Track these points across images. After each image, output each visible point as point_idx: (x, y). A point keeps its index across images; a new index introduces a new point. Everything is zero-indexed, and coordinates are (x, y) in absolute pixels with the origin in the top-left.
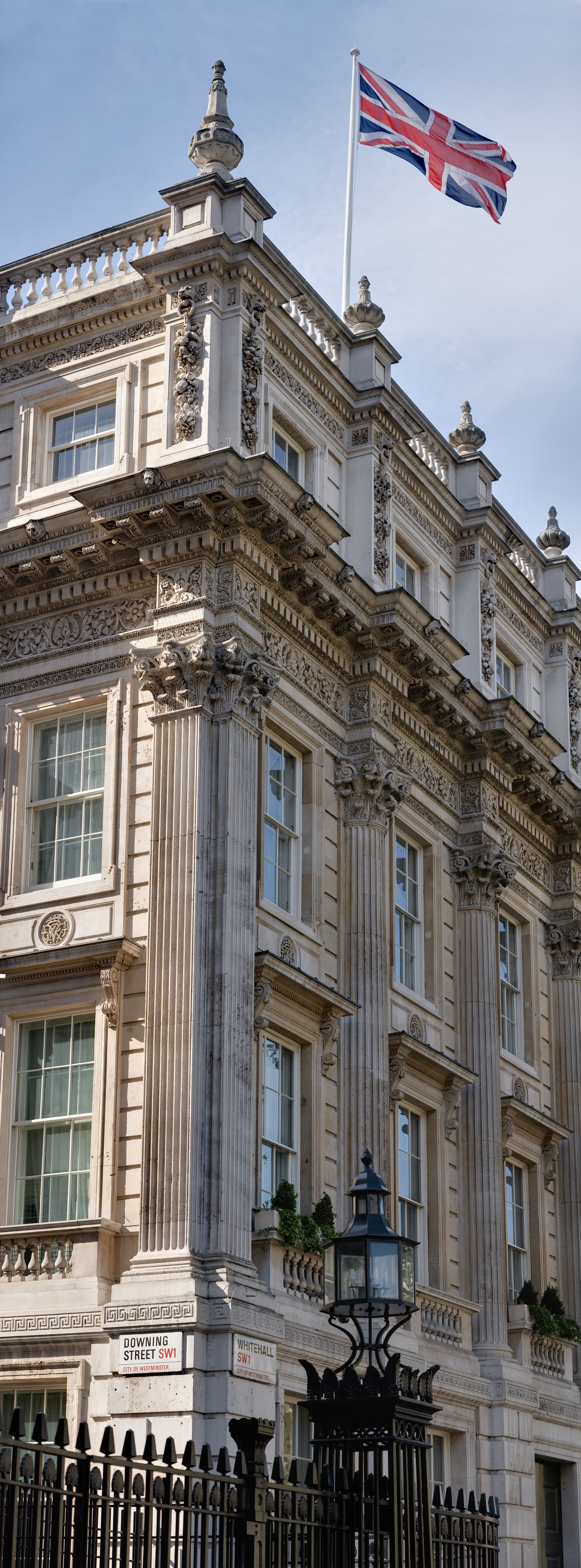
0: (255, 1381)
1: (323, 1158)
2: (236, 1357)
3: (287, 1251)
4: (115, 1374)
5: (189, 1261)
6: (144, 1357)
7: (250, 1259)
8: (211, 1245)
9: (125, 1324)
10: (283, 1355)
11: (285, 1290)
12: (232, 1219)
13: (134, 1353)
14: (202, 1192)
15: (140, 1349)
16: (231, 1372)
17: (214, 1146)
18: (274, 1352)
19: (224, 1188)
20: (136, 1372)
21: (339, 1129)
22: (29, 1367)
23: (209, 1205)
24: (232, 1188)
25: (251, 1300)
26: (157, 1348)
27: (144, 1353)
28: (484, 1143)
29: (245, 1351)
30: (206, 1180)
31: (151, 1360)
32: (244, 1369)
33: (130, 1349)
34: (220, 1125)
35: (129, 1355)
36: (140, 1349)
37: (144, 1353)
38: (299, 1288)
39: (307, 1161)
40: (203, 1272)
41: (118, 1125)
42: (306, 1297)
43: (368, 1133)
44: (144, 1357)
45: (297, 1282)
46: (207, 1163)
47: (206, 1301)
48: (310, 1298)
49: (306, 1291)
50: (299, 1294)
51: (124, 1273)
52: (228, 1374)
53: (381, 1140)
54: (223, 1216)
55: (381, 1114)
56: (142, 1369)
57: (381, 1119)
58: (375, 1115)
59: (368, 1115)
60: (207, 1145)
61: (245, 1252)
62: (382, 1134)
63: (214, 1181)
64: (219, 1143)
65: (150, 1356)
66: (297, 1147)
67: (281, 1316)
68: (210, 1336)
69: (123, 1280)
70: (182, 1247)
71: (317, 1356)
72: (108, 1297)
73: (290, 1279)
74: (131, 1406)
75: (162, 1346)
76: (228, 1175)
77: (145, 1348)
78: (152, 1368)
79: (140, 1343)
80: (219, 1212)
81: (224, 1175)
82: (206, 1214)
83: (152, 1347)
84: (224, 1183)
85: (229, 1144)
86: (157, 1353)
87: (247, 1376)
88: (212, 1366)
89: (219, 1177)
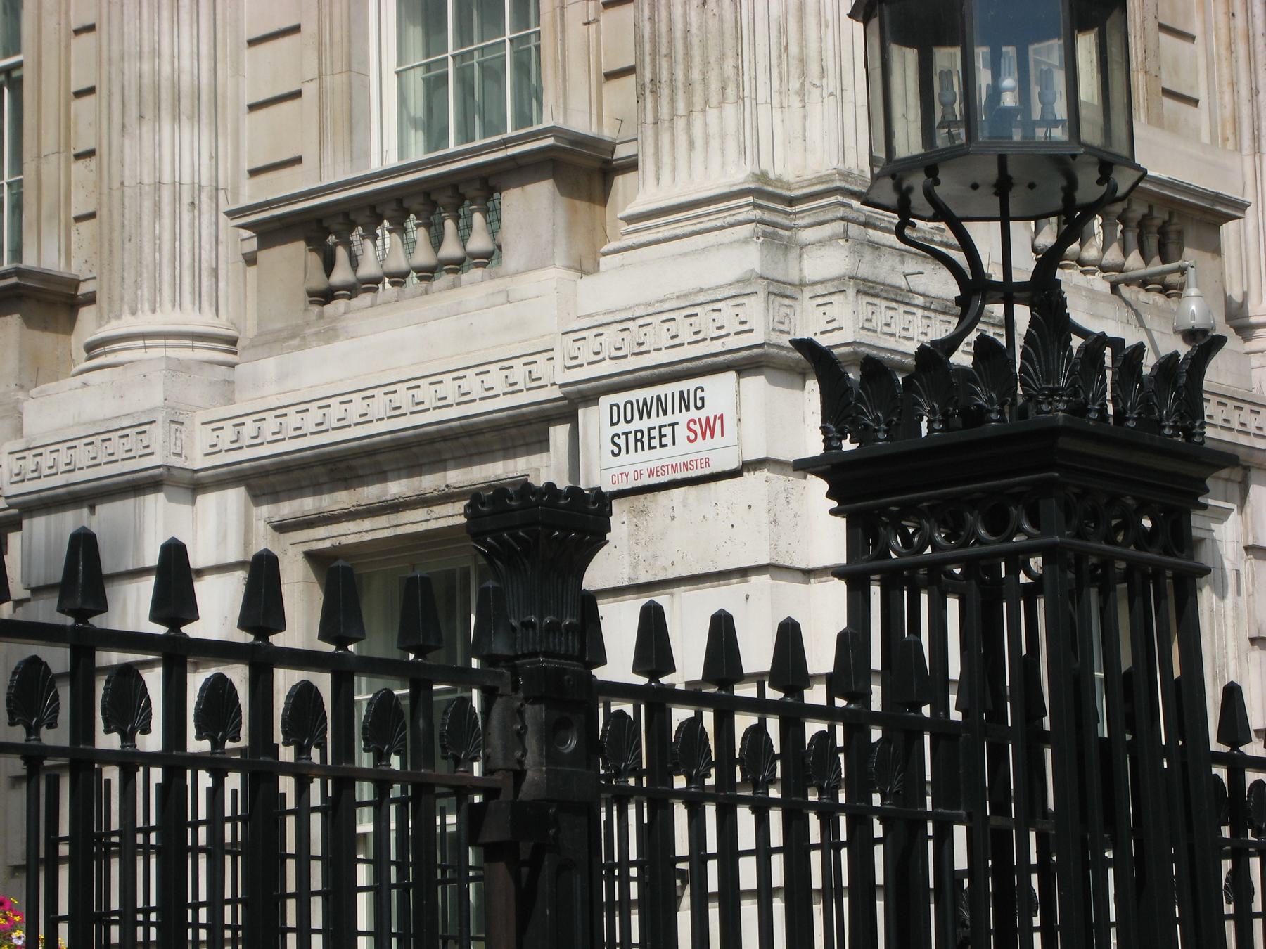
6: (655, 443)
9: (607, 368)
13: (631, 437)
15: (644, 424)
20: (639, 483)
22: (423, 501)
23: (802, 60)
25: (918, 283)
26: (682, 418)
27: (655, 433)
31: (670, 450)
33: (622, 427)
35: (622, 442)
36: (644, 424)
37: (655, 433)
44: (654, 443)
56: (651, 473)
74: (634, 567)
75: (694, 413)
77: (656, 421)
78: (674, 468)
79: (644, 409)
82: (795, 84)
86: (682, 431)
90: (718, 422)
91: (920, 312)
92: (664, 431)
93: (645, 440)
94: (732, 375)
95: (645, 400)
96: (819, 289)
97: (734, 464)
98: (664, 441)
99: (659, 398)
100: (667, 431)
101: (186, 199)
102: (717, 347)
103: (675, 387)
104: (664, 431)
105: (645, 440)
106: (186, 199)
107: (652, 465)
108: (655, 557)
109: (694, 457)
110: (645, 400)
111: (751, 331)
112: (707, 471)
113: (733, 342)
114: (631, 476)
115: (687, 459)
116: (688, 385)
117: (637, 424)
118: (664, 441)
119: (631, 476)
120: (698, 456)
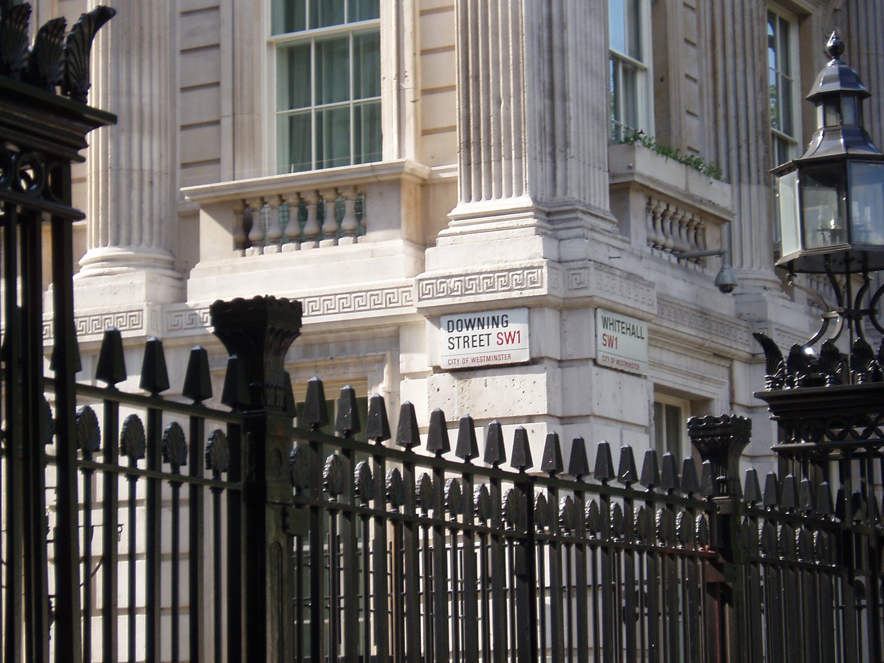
0: (622, 371)
1: (682, 76)
2: (600, 340)
3: (650, 199)
4: (437, 369)
5: (532, 213)
7: (608, 207)
8: (559, 191)
10: (657, 339)
11: (648, 250)
12: (584, 155)
13: (461, 340)
14: (542, 119)
15: (470, 332)
16: (595, 361)
17: (557, 55)
18: (645, 334)
19: (572, 112)
20: (466, 366)
21: (699, 37)
23: (553, 136)
24: (583, 112)
25: (615, 263)
26: (494, 330)
28: (873, 58)
29: (609, 332)
30: (547, 102)
32: (611, 356)
34: (563, 27)
35: (455, 342)
38: (664, 248)
39: (662, 80)
40: (549, 226)
41: (418, 32)
42: (674, 260)
43: (739, 40)
45: (661, 239)
46: (547, 79)
47: (557, 265)
48: (679, 260)
49: (673, 251)
50: (665, 256)
51: (441, 233)
52: (591, 363)
53: (756, 50)
54: (572, 151)
55: (755, 16)
56: (473, 360)
57: (755, 21)
58: (747, 17)
59: (738, 17)
60: (546, 56)
61: (601, 200)
62: (756, 42)
63: (558, 103)
64: (563, 51)
65: (484, 343)
66: (647, 61)
67: (651, 285)
68: (565, 313)
69: (440, 240)
70: (520, 193)
71: (691, 338)
72: (421, 265)
73: (653, 235)
75: (501, 329)
76: (577, 95)
77: (477, 331)
78: (489, 359)
79: (470, 325)
80: (566, 144)
81: (572, 95)
82: (548, 149)
83: (486, 330)
84: (572, 105)
85: (576, 52)
86: (493, 339)
87: (614, 366)
88: (571, 352)
89: (565, 98)
90: (517, 335)
91: (617, 278)
92: (482, 338)
93: (470, 341)
94: (525, 312)
95: (470, 320)
96: (573, 265)
97: (526, 359)
98: (482, 343)
99: (479, 319)
100: (484, 338)
101: (147, 179)
102: (515, 294)
103: (490, 314)
104: (482, 338)
105: (470, 341)
106: (147, 179)
107: (475, 356)
108: (473, 406)
109: (501, 353)
110: (470, 320)
111: (538, 287)
112: (509, 362)
113: (527, 293)
114: (461, 361)
115: (497, 354)
116: (500, 314)
117: (465, 332)
118: (482, 343)
119: (461, 361)
120: (504, 353)
